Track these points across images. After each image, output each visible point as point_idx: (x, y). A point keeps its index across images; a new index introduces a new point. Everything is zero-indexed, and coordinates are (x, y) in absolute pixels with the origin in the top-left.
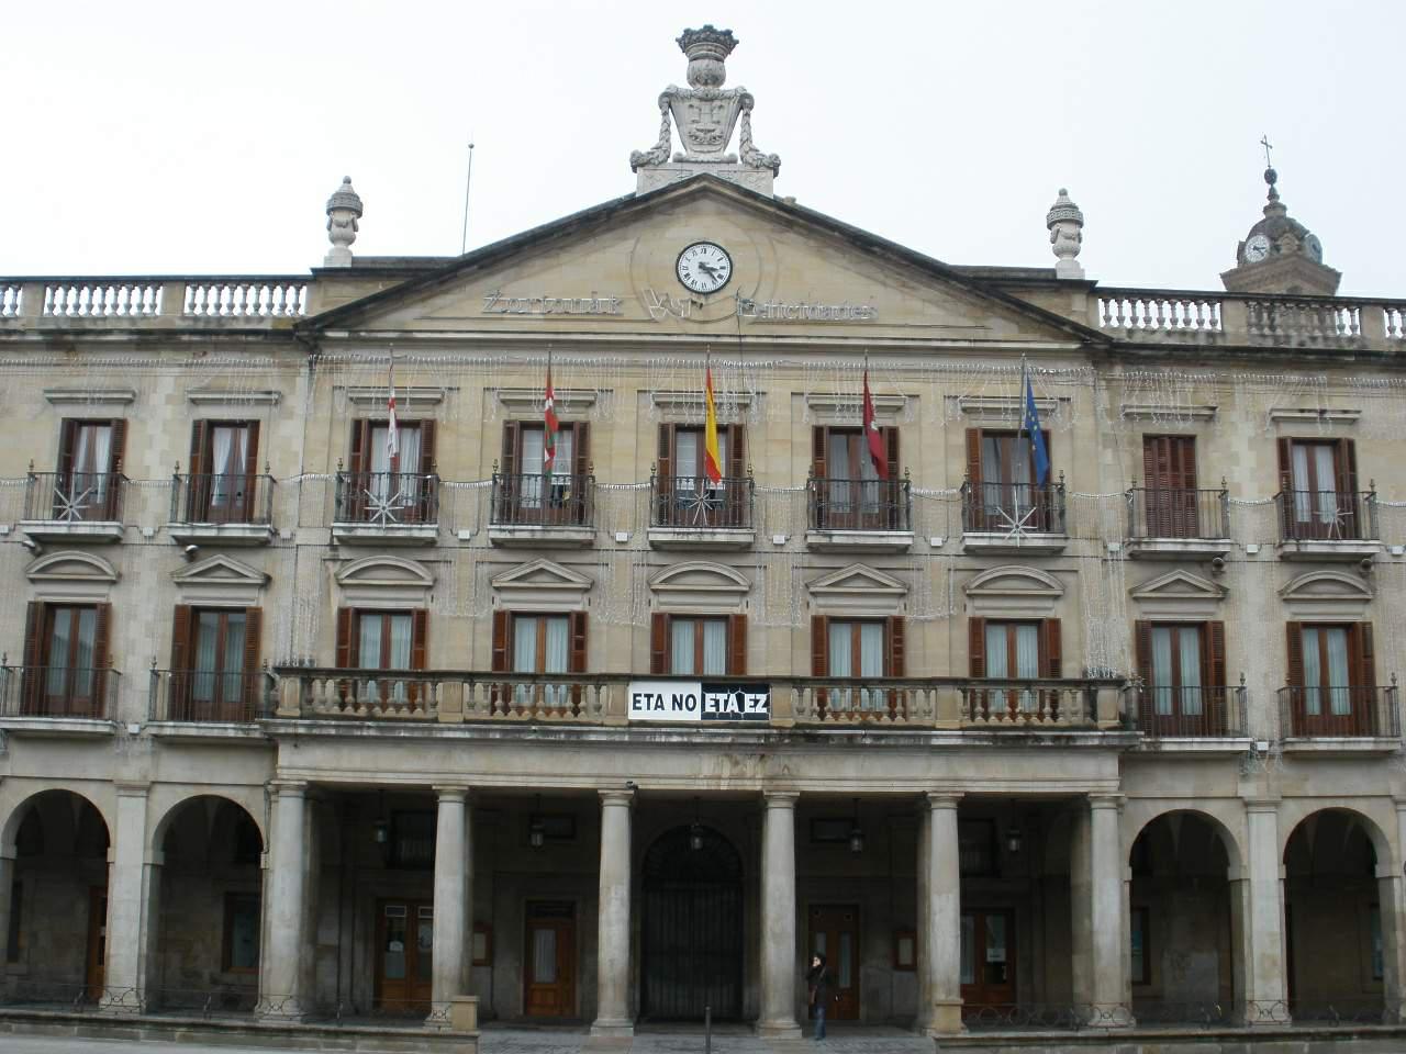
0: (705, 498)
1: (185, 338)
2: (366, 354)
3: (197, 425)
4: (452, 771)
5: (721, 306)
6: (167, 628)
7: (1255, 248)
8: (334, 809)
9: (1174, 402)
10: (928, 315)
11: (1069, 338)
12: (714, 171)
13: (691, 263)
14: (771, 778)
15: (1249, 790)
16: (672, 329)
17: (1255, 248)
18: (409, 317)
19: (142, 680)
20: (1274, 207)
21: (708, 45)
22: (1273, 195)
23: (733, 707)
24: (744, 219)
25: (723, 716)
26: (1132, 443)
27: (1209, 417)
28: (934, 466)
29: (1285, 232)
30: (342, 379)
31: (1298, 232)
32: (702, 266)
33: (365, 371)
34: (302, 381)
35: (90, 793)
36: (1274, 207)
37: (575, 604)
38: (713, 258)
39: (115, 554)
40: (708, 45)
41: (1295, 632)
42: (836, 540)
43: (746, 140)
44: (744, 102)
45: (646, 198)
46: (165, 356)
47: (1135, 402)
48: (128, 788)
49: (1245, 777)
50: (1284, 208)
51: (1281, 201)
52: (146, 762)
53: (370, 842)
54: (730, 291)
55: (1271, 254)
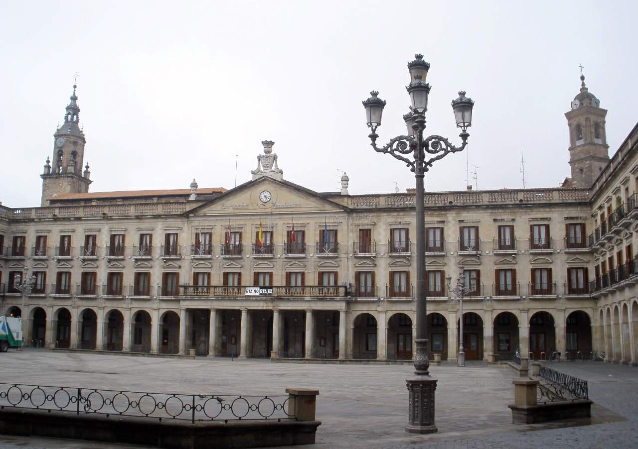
0: (264, 248)
1: (162, 216)
2: (197, 219)
3: (166, 234)
4: (213, 305)
5: (268, 205)
6: (161, 277)
7: (575, 104)
8: (191, 312)
9: (366, 222)
10: (312, 205)
11: (342, 209)
12: (267, 175)
13: (263, 196)
14: (274, 307)
15: (379, 309)
16: (259, 211)
17: (575, 104)
18: (206, 211)
19: (156, 288)
20: (584, 89)
21: (268, 144)
22: (583, 84)
23: (266, 292)
24: (274, 185)
25: (264, 294)
26: (357, 231)
27: (375, 224)
28: (312, 239)
29: (585, 98)
30: (193, 224)
31: (591, 97)
32: (265, 196)
33: (199, 223)
34: (186, 225)
35: (147, 310)
36: (584, 89)
37: (238, 270)
38: (267, 194)
39: (150, 262)
40: (268, 144)
41: (392, 274)
42: (289, 256)
43: (276, 166)
44: (275, 157)
45: (254, 181)
46: (159, 220)
47: (356, 222)
48: (155, 309)
49: (378, 306)
50: (587, 89)
51: (586, 87)
52: (158, 304)
53: (199, 318)
54: (271, 202)
55: (580, 106)
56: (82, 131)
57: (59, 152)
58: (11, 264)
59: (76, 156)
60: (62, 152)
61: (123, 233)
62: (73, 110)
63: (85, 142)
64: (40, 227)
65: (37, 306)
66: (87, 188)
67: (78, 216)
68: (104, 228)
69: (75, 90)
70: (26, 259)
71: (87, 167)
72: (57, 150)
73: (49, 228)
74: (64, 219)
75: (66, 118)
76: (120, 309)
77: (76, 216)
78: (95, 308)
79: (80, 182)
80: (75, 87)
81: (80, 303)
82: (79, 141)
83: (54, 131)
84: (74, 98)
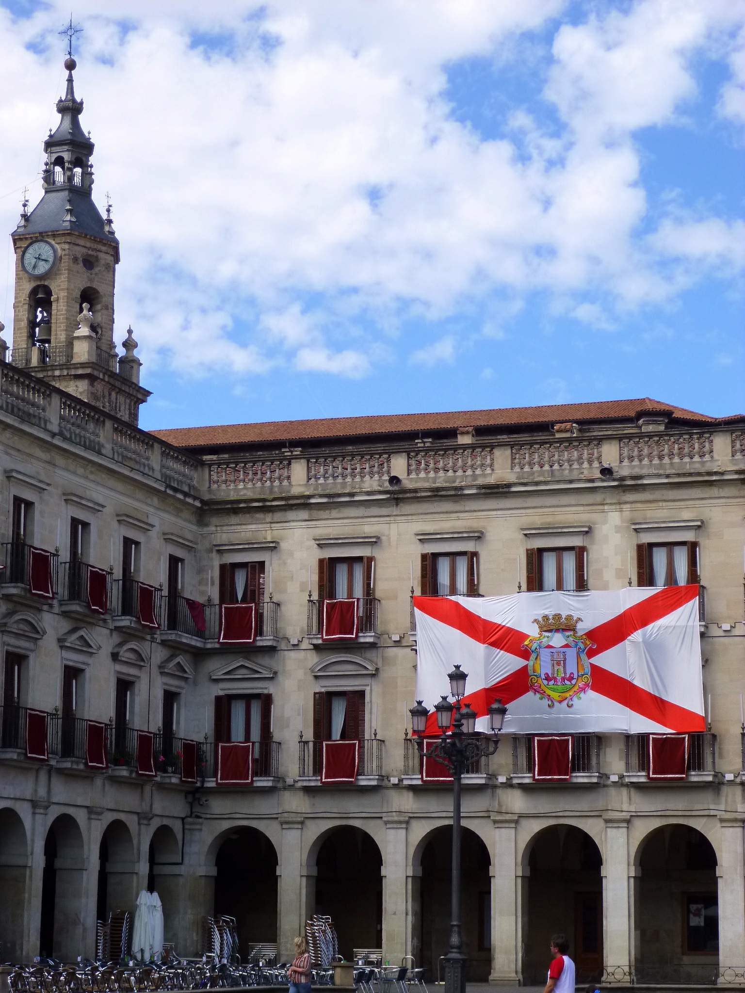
56: (110, 222)
57: (34, 292)
58: (217, 667)
59: (94, 298)
60: (49, 293)
61: (689, 536)
62: (71, 148)
63: (117, 260)
64: (335, 526)
65: (338, 823)
66: (135, 416)
67: (492, 480)
68: (605, 522)
69: (70, 80)
70: (283, 646)
71: (129, 344)
72: (28, 287)
73: (369, 528)
74: (437, 494)
75: (48, 176)
76: (697, 824)
77: (480, 481)
78: (590, 821)
79: (113, 394)
80: (71, 66)
81: (516, 802)
82: (101, 255)
83: (14, 222)
84: (71, 108)
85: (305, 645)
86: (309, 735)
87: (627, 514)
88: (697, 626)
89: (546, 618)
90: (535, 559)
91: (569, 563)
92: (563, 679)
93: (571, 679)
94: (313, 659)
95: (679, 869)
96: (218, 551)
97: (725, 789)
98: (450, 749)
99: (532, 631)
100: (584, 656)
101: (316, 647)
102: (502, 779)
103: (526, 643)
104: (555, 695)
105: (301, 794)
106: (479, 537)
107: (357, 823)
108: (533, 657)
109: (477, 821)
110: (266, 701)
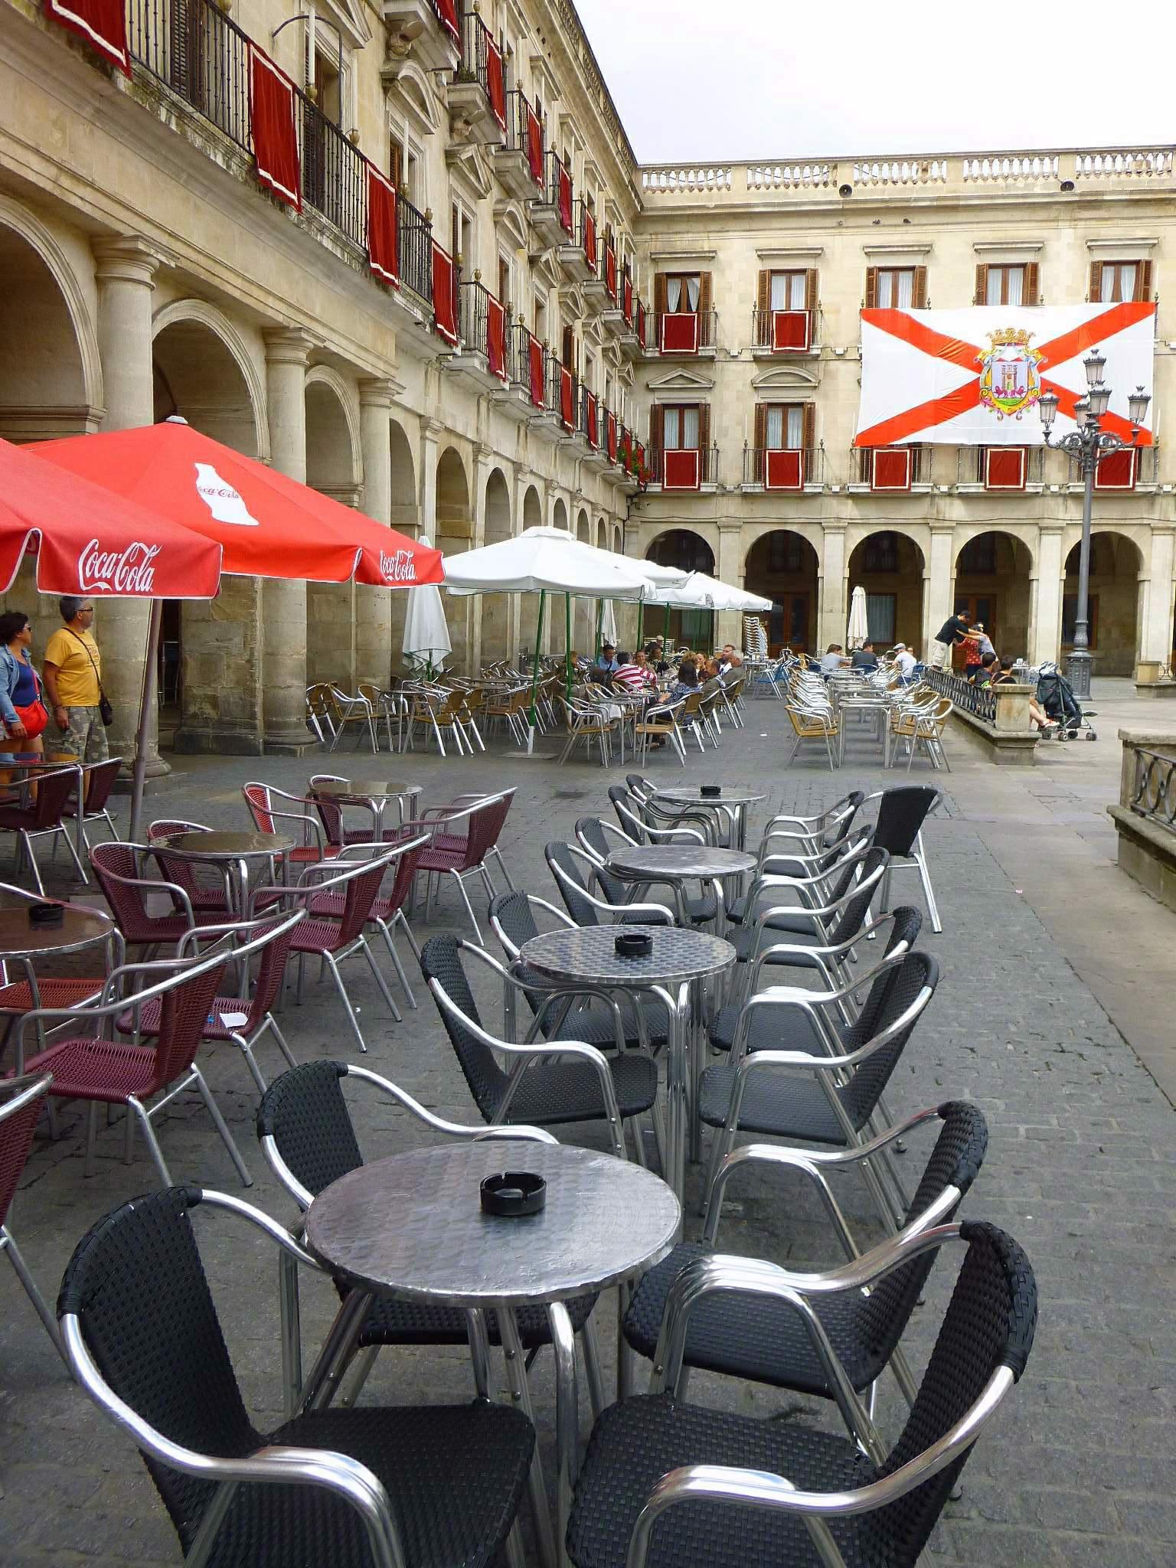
58: (655, 377)
70: (720, 357)
73: (812, 239)
76: (1128, 532)
78: (1025, 528)
81: (957, 510)
85: (742, 358)
86: (751, 445)
87: (1080, 232)
88: (1150, 343)
89: (999, 332)
90: (982, 274)
91: (1016, 279)
92: (1013, 392)
93: (1021, 392)
94: (753, 371)
95: (1108, 571)
96: (653, 260)
97: (1159, 500)
98: (888, 461)
99: (984, 344)
100: (1034, 370)
101: (757, 359)
102: (944, 488)
103: (979, 357)
104: (1005, 408)
105: (739, 500)
106: (926, 251)
107: (794, 528)
108: (986, 369)
109: (914, 527)
110: (702, 412)
